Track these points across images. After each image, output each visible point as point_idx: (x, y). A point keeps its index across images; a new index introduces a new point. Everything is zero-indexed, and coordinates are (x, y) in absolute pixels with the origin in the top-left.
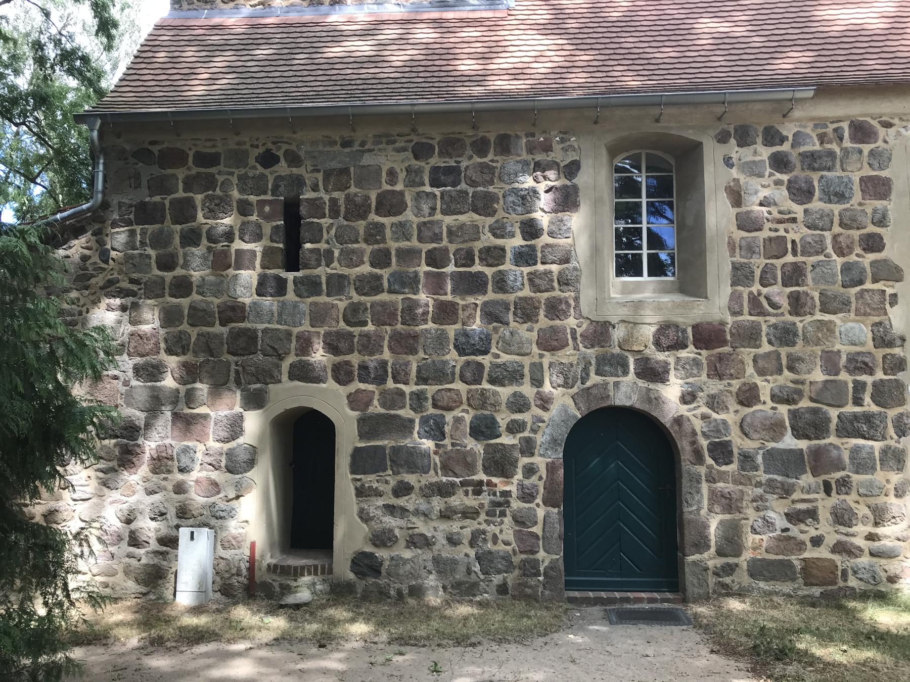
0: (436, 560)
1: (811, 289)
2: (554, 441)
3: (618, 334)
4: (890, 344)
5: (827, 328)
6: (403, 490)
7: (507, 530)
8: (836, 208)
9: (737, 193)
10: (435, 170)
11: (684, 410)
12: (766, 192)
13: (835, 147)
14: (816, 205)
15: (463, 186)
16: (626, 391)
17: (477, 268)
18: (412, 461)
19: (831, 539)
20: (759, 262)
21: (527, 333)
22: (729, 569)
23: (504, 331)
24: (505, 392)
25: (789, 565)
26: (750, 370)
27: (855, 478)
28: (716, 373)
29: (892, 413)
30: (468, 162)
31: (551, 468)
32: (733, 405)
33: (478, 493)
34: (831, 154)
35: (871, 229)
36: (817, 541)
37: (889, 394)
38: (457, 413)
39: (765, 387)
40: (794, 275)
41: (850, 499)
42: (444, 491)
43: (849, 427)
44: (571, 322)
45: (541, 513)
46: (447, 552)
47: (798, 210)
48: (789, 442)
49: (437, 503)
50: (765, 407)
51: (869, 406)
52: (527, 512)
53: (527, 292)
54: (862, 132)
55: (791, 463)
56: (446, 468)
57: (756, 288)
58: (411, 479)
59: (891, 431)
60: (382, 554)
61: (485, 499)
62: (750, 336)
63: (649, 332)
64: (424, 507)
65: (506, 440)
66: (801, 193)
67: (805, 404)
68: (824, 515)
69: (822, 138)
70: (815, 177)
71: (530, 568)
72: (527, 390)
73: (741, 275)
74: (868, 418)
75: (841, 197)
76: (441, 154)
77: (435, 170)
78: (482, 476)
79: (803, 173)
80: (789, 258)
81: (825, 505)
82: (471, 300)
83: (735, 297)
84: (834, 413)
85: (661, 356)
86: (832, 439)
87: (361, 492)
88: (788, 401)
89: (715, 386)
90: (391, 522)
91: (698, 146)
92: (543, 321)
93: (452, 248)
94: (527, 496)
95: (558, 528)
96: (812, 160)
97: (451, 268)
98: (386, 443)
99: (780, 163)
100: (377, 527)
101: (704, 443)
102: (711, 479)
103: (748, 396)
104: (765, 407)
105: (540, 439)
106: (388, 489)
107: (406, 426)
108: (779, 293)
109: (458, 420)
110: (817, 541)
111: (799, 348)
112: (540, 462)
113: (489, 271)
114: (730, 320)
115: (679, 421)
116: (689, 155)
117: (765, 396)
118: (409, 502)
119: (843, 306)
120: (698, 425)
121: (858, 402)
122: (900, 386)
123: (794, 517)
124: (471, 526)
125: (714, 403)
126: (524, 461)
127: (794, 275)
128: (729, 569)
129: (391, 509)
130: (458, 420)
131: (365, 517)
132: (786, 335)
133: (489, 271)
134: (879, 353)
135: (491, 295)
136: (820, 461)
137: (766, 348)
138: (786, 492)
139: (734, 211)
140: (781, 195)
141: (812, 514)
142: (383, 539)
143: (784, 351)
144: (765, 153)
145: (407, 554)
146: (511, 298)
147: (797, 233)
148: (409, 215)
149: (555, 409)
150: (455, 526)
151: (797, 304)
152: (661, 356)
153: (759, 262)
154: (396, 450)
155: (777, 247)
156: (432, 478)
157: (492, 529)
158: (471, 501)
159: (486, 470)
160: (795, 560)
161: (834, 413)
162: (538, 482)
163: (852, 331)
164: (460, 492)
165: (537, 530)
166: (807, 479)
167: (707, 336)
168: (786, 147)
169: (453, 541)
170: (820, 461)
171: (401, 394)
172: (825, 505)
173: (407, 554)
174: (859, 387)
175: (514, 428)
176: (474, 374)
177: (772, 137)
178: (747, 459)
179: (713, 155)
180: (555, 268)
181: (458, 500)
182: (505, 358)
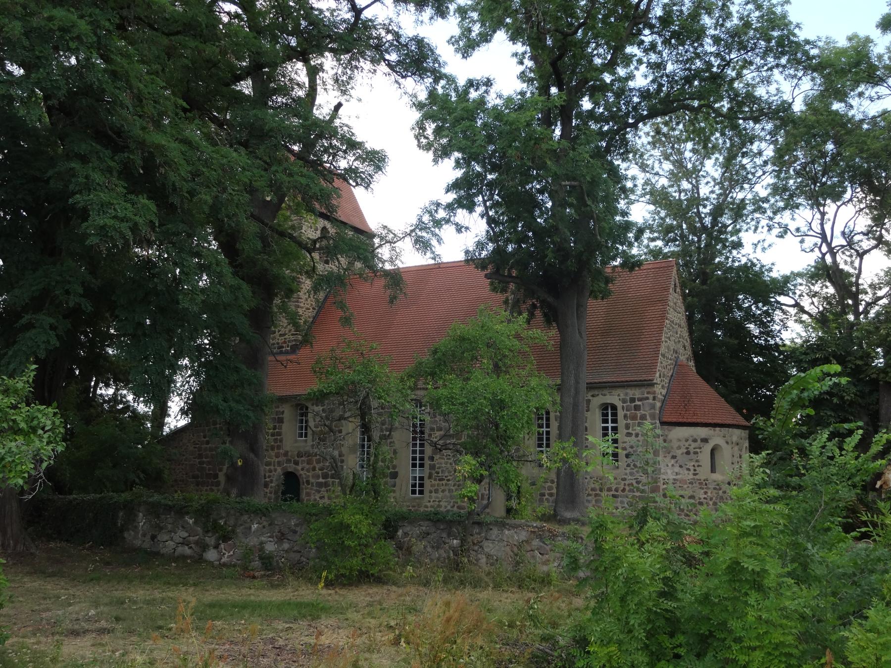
11: (302, 472)
16: (291, 467)
21: (273, 453)
24: (268, 468)
39: (317, 466)
48: (321, 480)
55: (320, 485)
65: (267, 479)
72: (272, 467)
81: (326, 495)
89: (308, 467)
94: (271, 493)
103: (314, 469)
136: (326, 485)
138: (319, 492)
166: (323, 489)
167: (308, 454)
172: (326, 495)
175: (269, 477)
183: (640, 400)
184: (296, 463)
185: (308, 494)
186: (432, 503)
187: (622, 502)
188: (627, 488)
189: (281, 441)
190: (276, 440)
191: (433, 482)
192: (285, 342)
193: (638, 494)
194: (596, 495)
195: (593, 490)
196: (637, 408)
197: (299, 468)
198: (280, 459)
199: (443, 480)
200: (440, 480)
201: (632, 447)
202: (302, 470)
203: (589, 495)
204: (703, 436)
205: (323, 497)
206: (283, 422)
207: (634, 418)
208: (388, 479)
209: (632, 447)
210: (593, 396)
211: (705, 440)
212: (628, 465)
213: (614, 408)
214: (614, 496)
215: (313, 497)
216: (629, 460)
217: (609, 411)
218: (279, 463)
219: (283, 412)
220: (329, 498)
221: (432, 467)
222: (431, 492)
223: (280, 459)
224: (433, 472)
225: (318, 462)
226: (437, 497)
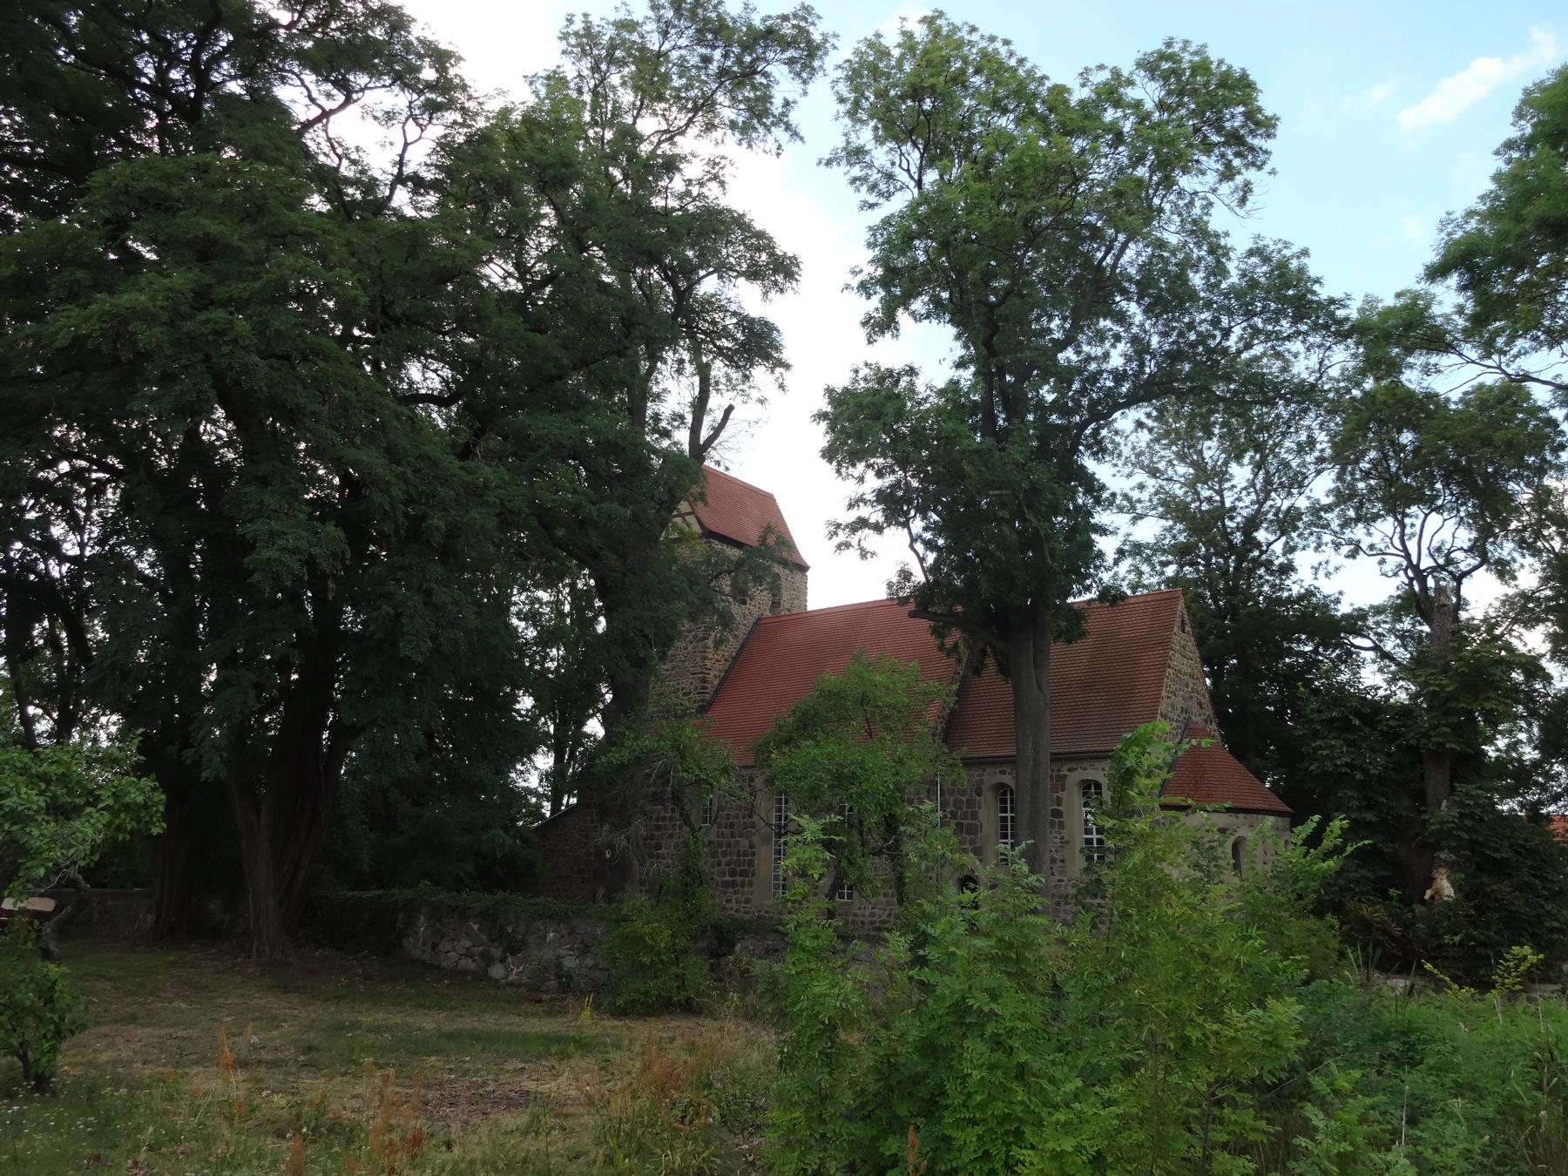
1: (736, 830)
37: (751, 864)
39: (723, 861)
55: (726, 884)
89: (711, 860)
103: (719, 864)
132: (729, 845)
136: (734, 884)
151: (732, 835)
163: (744, 842)
204: (1221, 825)
211: (1222, 831)
213: (1098, 786)
220: (738, 901)
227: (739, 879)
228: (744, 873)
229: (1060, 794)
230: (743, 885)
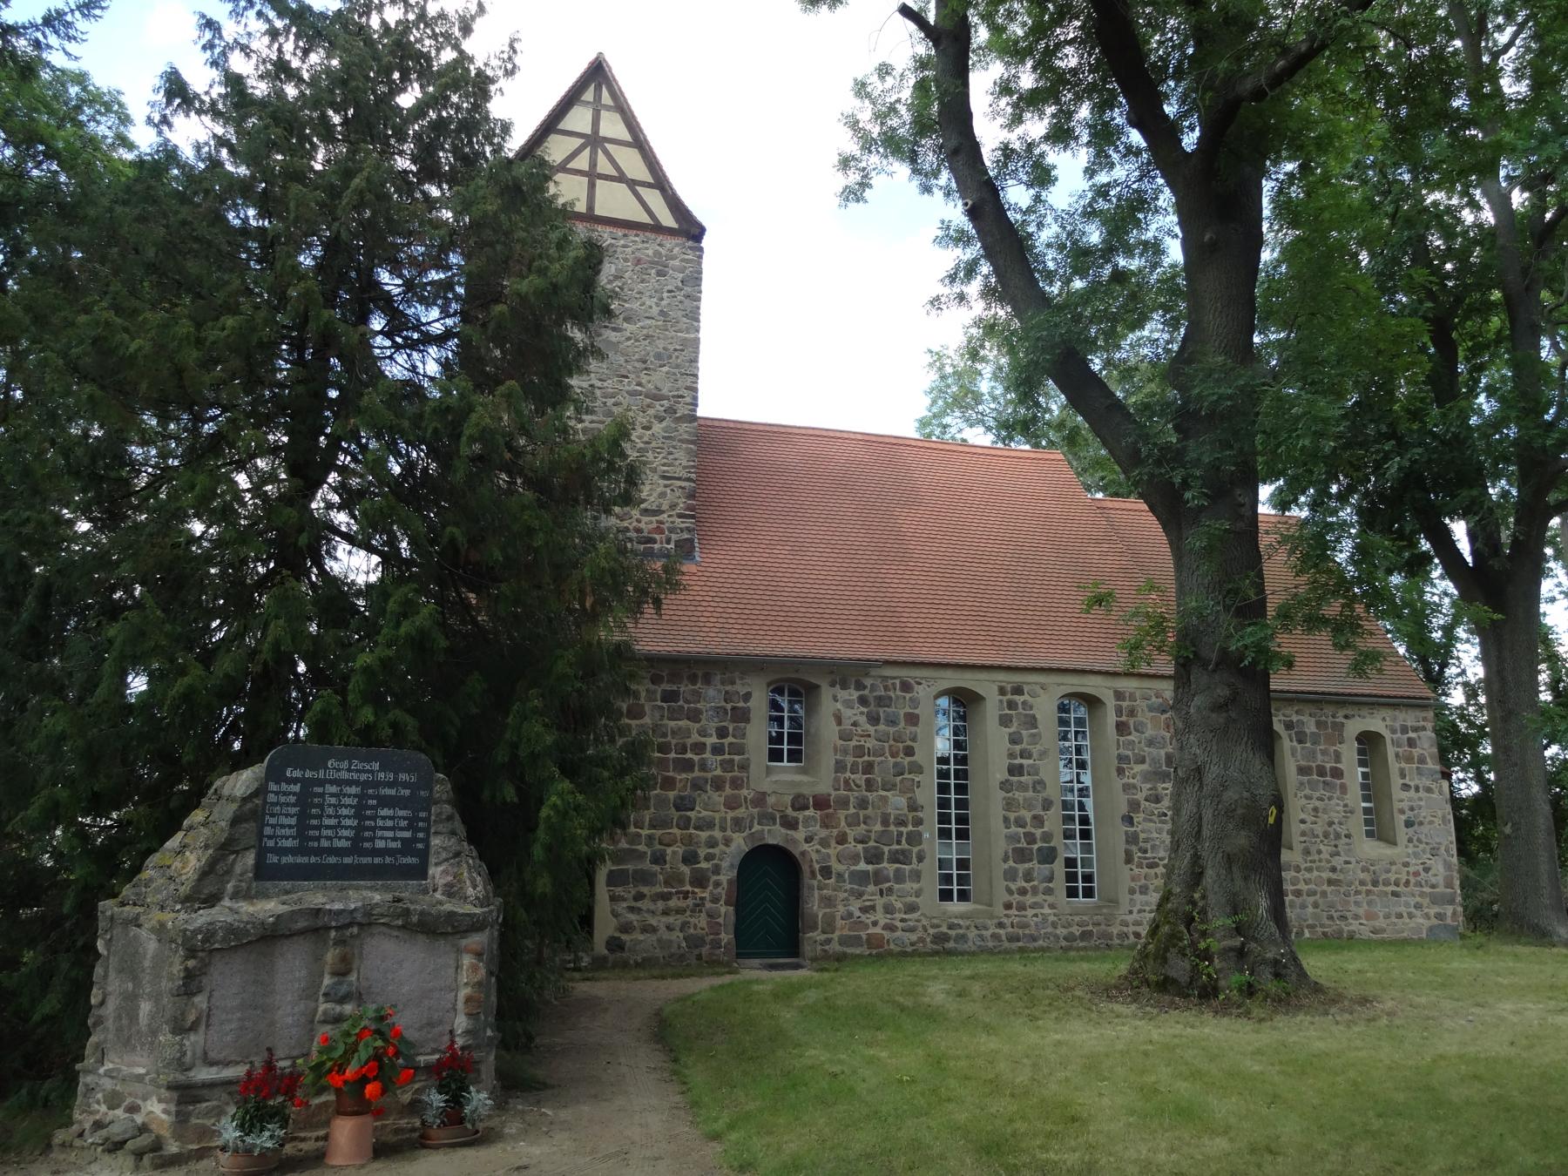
0: (659, 941)
2: (732, 866)
3: (771, 800)
4: (915, 810)
5: (884, 799)
6: (640, 897)
7: (702, 921)
8: (892, 730)
9: (836, 713)
10: (664, 691)
11: (806, 847)
12: (855, 714)
13: (891, 694)
14: (882, 727)
15: (681, 703)
16: (775, 835)
17: (689, 755)
18: (644, 878)
19: (882, 922)
20: (850, 759)
21: (718, 798)
22: (829, 941)
23: (705, 797)
24: (704, 835)
25: (859, 937)
26: (843, 823)
27: (896, 886)
28: (825, 825)
29: (915, 850)
30: (685, 688)
31: (730, 882)
32: (833, 843)
33: (685, 898)
34: (890, 698)
35: (909, 743)
36: (875, 924)
38: (674, 848)
39: (851, 834)
40: (869, 767)
41: (892, 898)
42: (666, 897)
43: (894, 859)
44: (745, 792)
45: (723, 910)
46: (666, 935)
47: (871, 729)
48: (862, 866)
49: (660, 905)
50: (851, 846)
51: (904, 845)
52: (717, 912)
53: (718, 772)
54: (906, 687)
55: (862, 878)
56: (667, 883)
57: (848, 774)
58: (645, 890)
59: (915, 860)
60: (624, 937)
61: (690, 902)
62: (844, 803)
63: (788, 799)
64: (652, 907)
65: (704, 865)
66: (874, 720)
67: (872, 843)
68: (879, 909)
69: (886, 688)
70: (881, 710)
71: (716, 944)
72: (717, 834)
73: (840, 767)
74: (903, 852)
75: (893, 723)
76: (669, 682)
77: (664, 691)
78: (688, 888)
79: (876, 707)
80: (866, 758)
81: (880, 902)
82: (684, 776)
83: (837, 780)
84: (886, 849)
85: (795, 814)
86: (885, 864)
87: (613, 899)
88: (862, 842)
89: (824, 833)
90: (632, 917)
91: (818, 687)
92: (728, 791)
93: (674, 742)
95: (733, 918)
96: (881, 701)
97: (673, 755)
98: (630, 867)
99: (863, 701)
100: (622, 920)
101: (817, 867)
102: (820, 889)
103: (842, 839)
104: (851, 846)
105: (725, 864)
106: (630, 896)
107: (642, 855)
108: (860, 778)
109: (674, 853)
110: (875, 924)
111: (870, 811)
112: (723, 878)
113: (696, 758)
114: (833, 793)
115: (803, 853)
116: (813, 689)
117: (850, 839)
118: (644, 904)
119: (892, 787)
120: (814, 856)
121: (899, 843)
122: (920, 834)
123: (864, 910)
124: (681, 919)
125: (824, 843)
126: (715, 878)
127: (869, 767)
128: (829, 941)
129: (631, 909)
130: (674, 853)
131: (615, 915)
132: (863, 804)
133: (696, 758)
134: (910, 815)
135: (697, 773)
136: (878, 878)
137: (852, 811)
138: (860, 895)
139: (837, 729)
140: (863, 719)
141: (873, 908)
142: (626, 928)
143: (862, 813)
144: (855, 695)
145: (641, 937)
146: (709, 775)
147: (870, 744)
148: (647, 720)
149: (733, 846)
150: (671, 919)
151: (870, 785)
152: (795, 814)
153: (850, 759)
154: (635, 871)
155: (860, 751)
156: (658, 889)
157: (692, 920)
158: (682, 904)
159: (692, 884)
160: (863, 935)
161: (886, 849)
162: (722, 892)
163: (897, 802)
164: (675, 898)
165: (721, 920)
166: (871, 888)
167: (821, 803)
168: (866, 692)
169: (669, 928)
170: (878, 878)
171: (639, 835)
173: (641, 937)
174: (900, 834)
175: (709, 858)
176: (685, 824)
177: (860, 686)
178: (840, 875)
179: (826, 693)
180: (736, 758)
181: (673, 903)
182: (704, 813)
183: (1415, 730)
184: (791, 824)
185: (828, 902)
186: (1135, 916)
187: (1407, 905)
188: (1412, 880)
189: (744, 767)
190: (727, 765)
191: (1136, 871)
192: (659, 530)
193: (1427, 890)
194: (1368, 892)
195: (1362, 883)
196: (1411, 743)
197: (800, 835)
198: (741, 812)
199: (1157, 865)
200: (1150, 866)
201: (1412, 809)
202: (806, 841)
203: (1357, 893)
205: (873, 908)
206: (748, 720)
207: (1409, 759)
208: (1034, 864)
209: (1412, 809)
210: (1346, 717)
212: (1410, 840)
214: (1395, 894)
215: (841, 909)
216: (1411, 830)
217: (1369, 743)
218: (738, 824)
219: (747, 697)
220: (889, 909)
221: (1132, 839)
222: (1132, 891)
223: (741, 812)
224: (1134, 848)
225: (853, 822)
226: (1147, 904)
227: (889, 868)
228: (899, 857)
229: (1338, 747)
230: (899, 877)
